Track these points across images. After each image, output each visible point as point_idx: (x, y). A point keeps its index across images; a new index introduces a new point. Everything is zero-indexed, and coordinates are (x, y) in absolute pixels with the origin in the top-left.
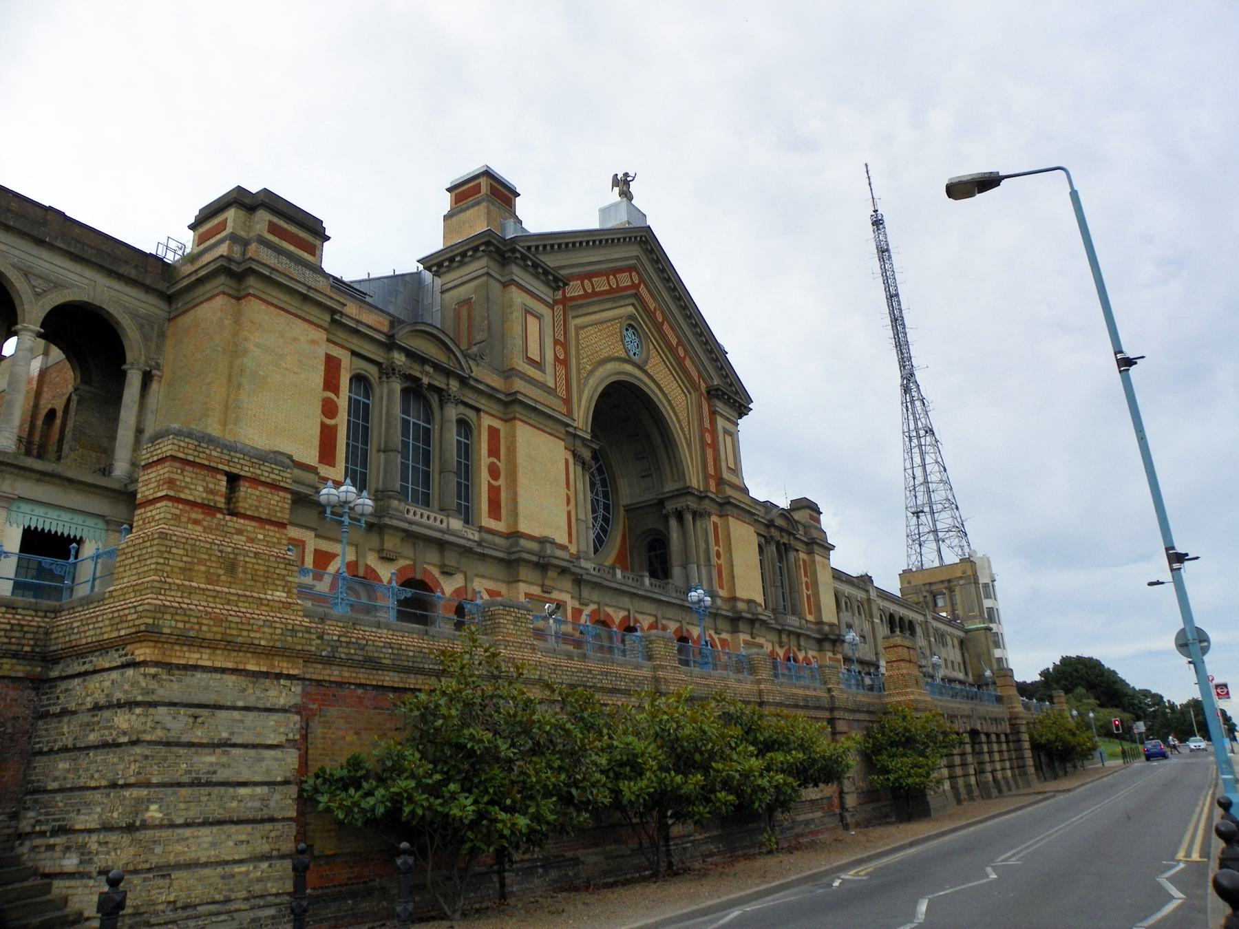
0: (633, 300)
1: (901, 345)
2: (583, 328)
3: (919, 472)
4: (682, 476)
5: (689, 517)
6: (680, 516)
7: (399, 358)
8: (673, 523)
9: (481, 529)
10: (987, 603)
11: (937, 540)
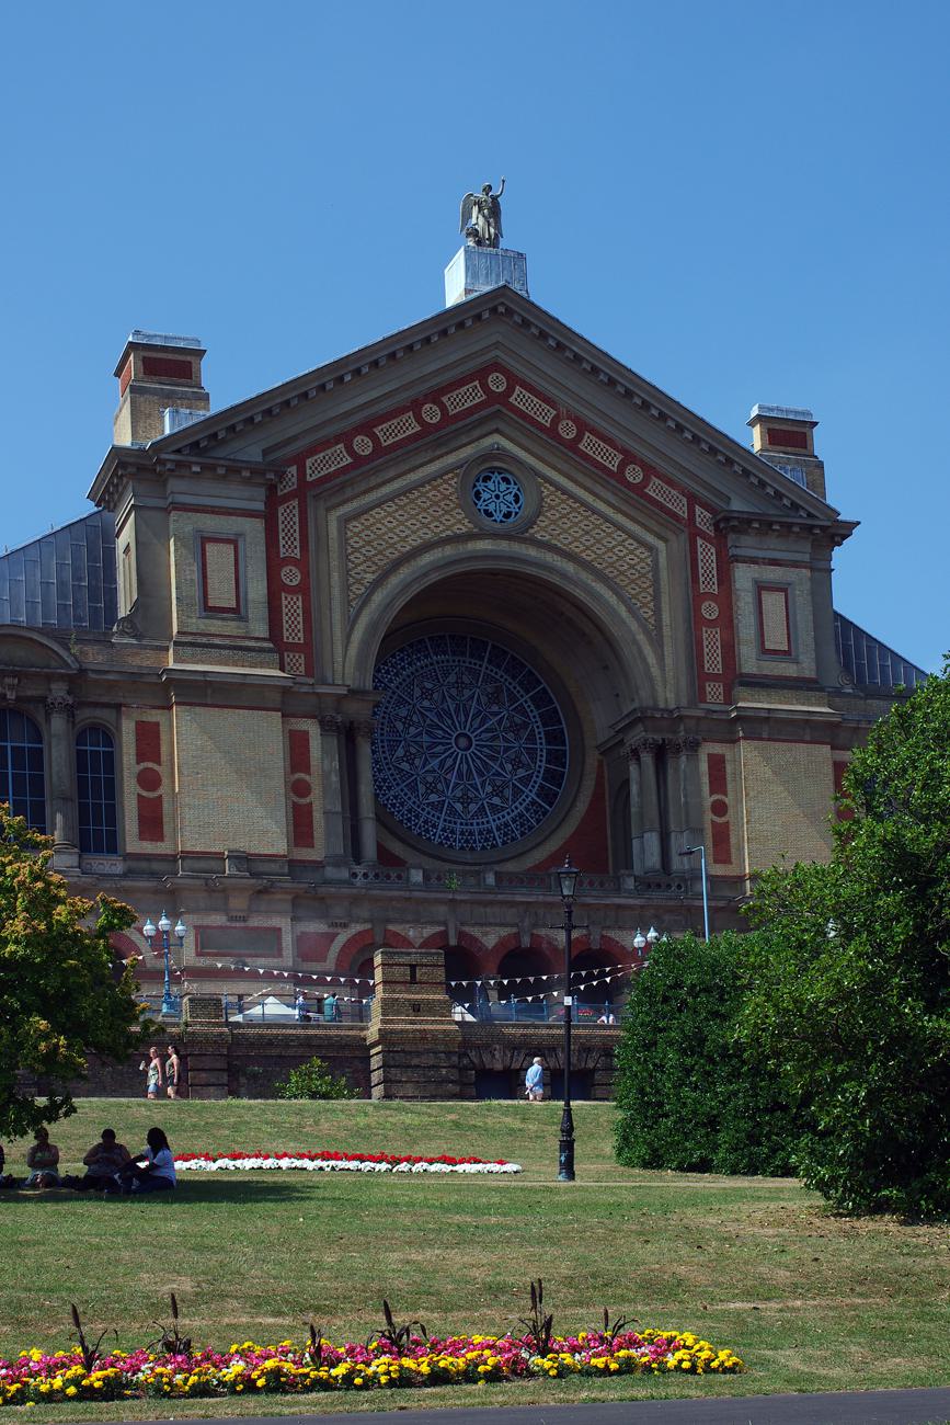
0: (502, 426)
2: (356, 516)
9: (128, 857)
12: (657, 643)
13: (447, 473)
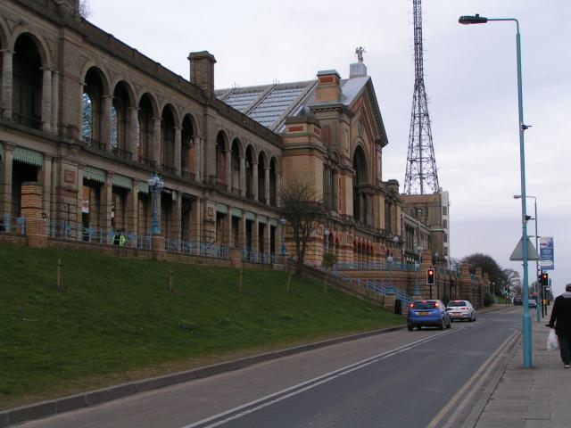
1: (419, 61)
3: (416, 138)
4: (367, 180)
5: (368, 196)
6: (364, 196)
7: (330, 162)
8: (361, 198)
10: (444, 217)
11: (421, 178)
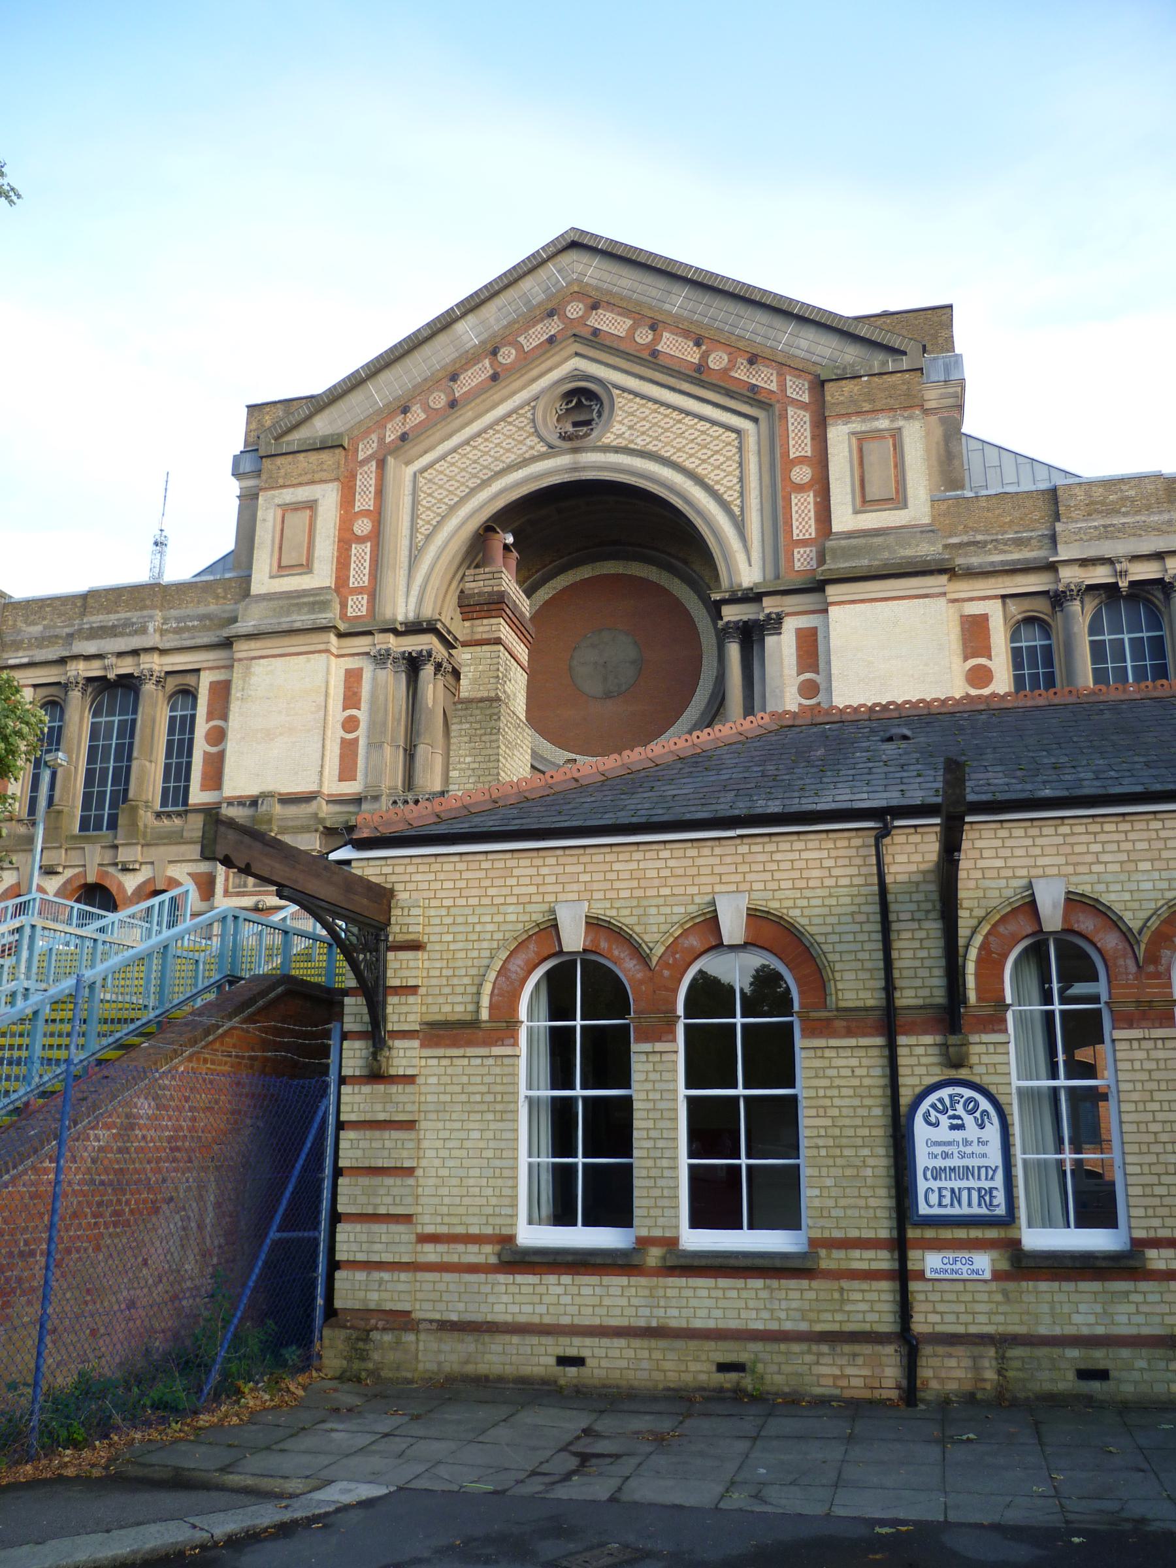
12: (740, 526)
13: (522, 407)
